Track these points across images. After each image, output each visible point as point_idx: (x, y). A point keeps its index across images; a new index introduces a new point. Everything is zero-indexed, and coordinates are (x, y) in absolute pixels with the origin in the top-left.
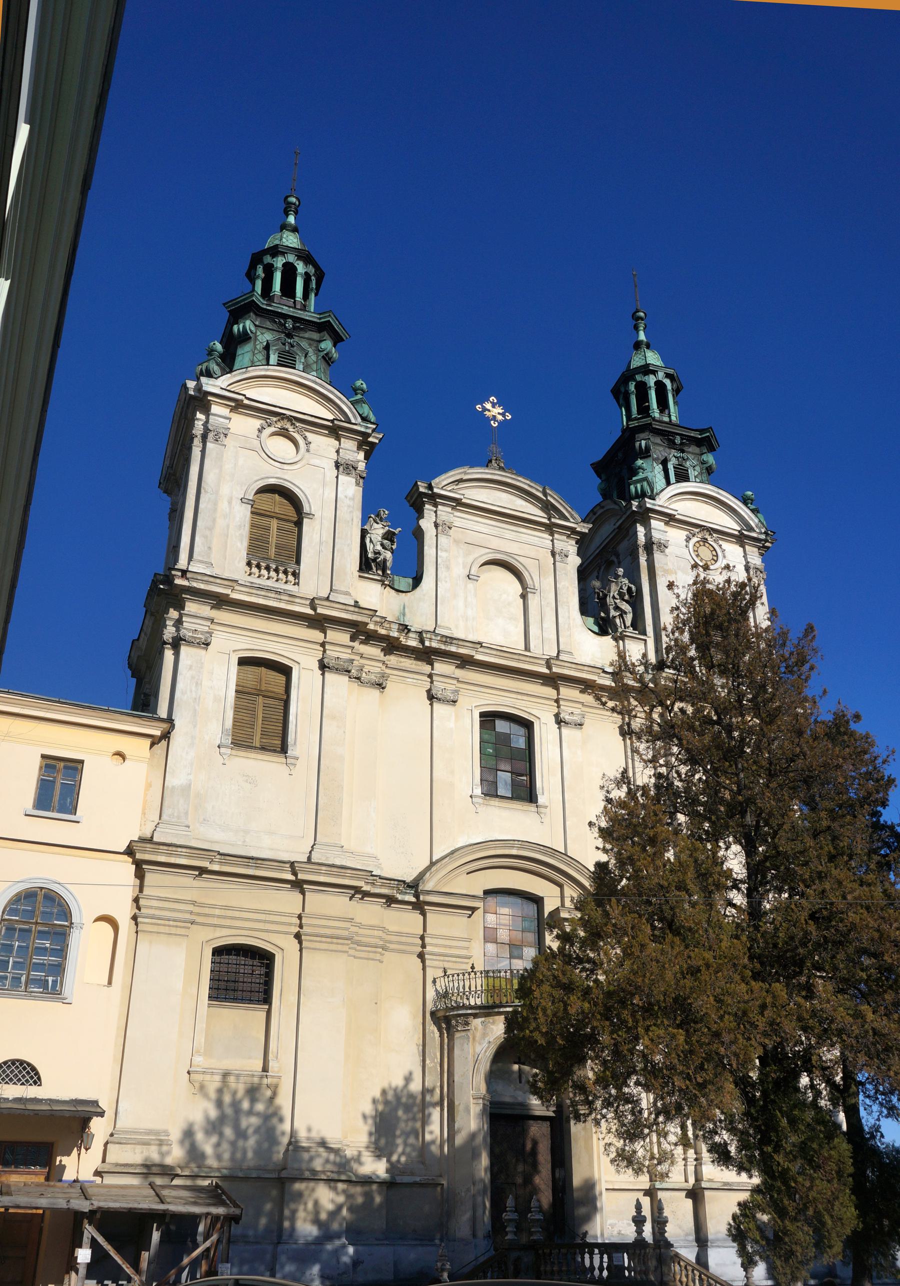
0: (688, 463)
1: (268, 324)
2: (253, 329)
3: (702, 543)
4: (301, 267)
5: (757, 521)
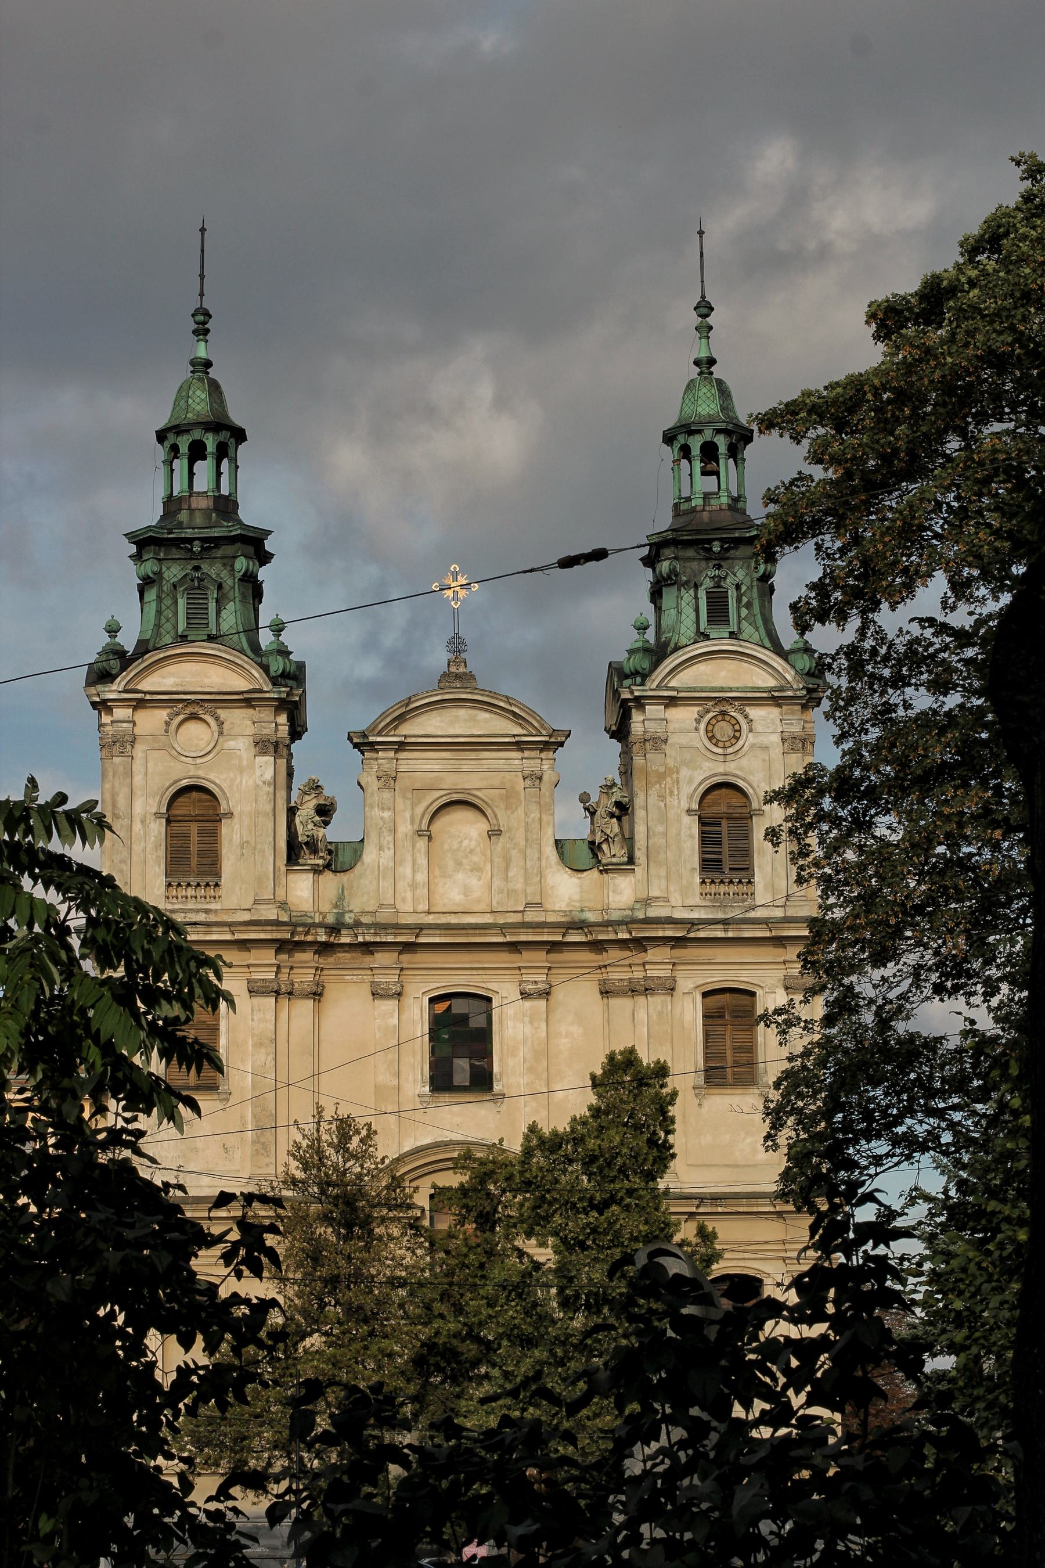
0: (728, 580)
1: (176, 553)
2: (155, 569)
3: (720, 718)
5: (793, 673)
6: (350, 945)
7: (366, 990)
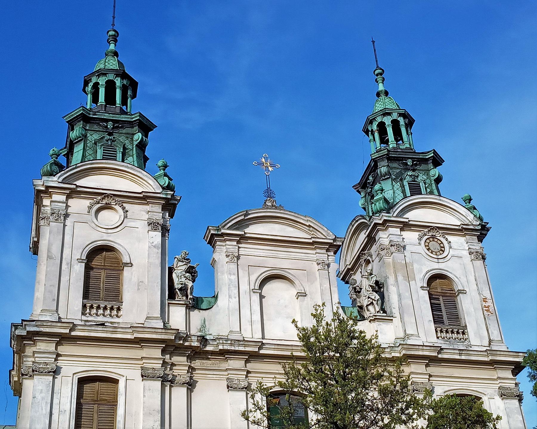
0: (419, 179)
1: (96, 127)
3: (431, 239)
4: (118, 82)
5: (472, 216)
6: (213, 353)
7: (225, 383)
